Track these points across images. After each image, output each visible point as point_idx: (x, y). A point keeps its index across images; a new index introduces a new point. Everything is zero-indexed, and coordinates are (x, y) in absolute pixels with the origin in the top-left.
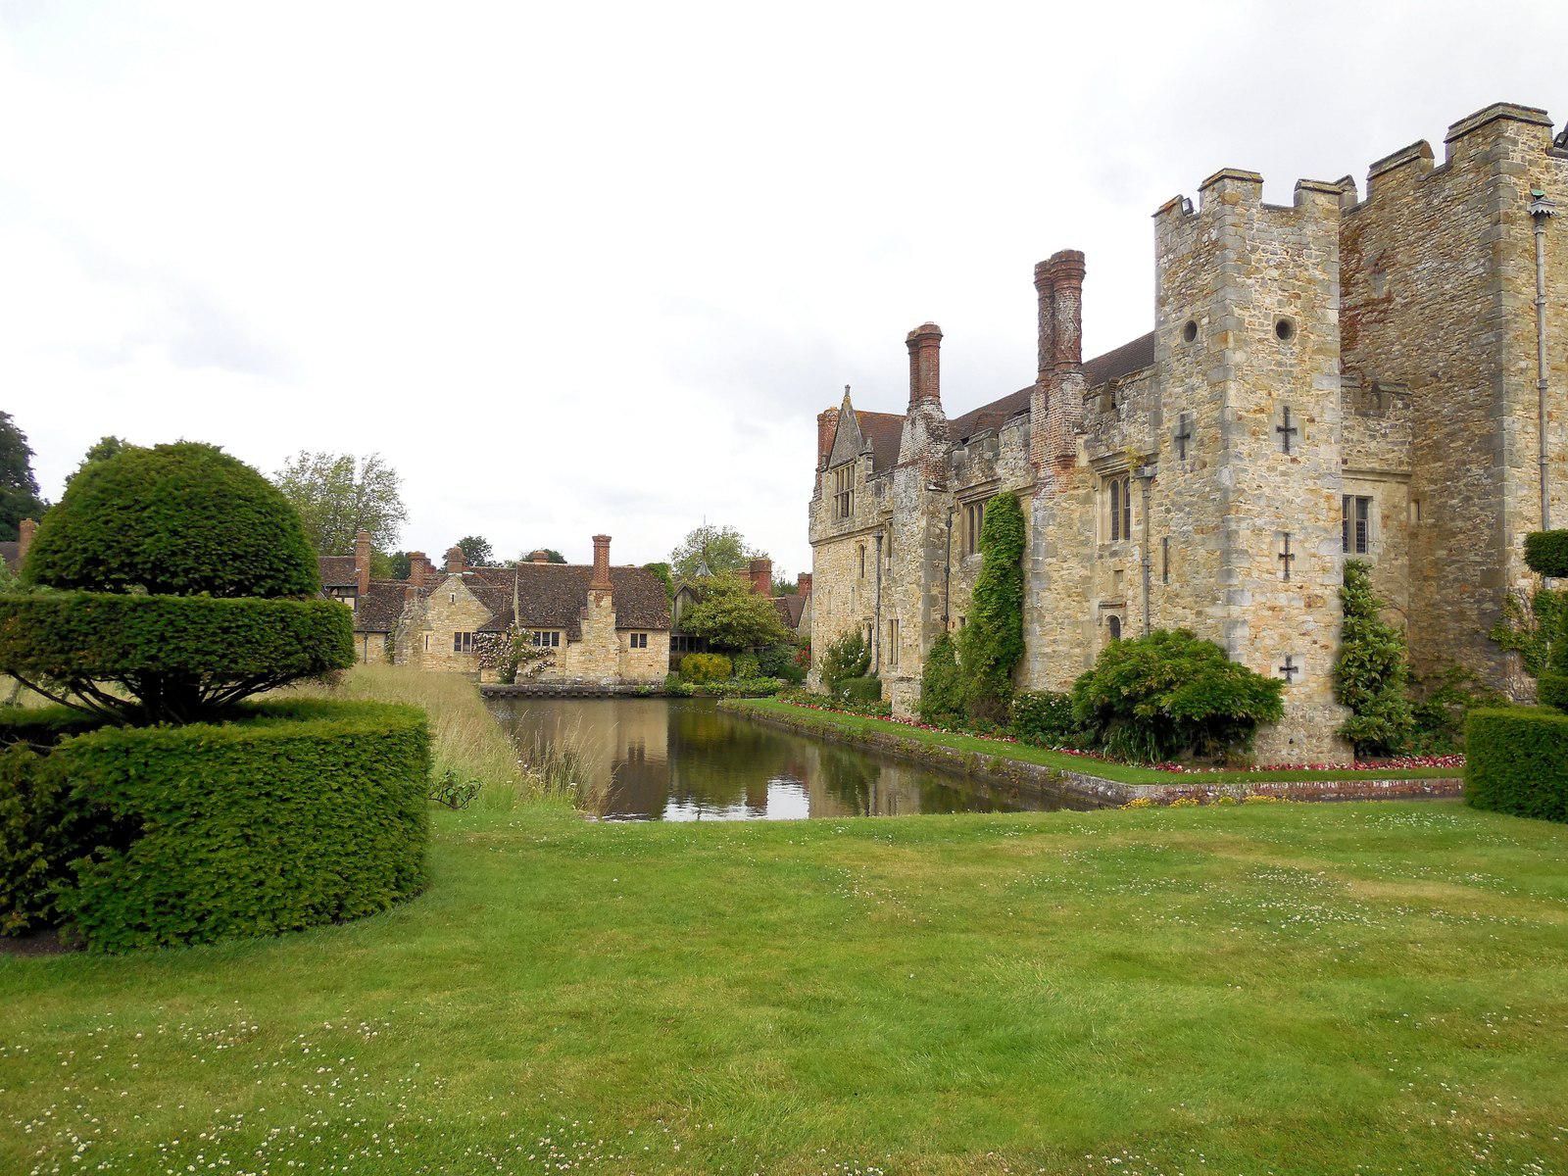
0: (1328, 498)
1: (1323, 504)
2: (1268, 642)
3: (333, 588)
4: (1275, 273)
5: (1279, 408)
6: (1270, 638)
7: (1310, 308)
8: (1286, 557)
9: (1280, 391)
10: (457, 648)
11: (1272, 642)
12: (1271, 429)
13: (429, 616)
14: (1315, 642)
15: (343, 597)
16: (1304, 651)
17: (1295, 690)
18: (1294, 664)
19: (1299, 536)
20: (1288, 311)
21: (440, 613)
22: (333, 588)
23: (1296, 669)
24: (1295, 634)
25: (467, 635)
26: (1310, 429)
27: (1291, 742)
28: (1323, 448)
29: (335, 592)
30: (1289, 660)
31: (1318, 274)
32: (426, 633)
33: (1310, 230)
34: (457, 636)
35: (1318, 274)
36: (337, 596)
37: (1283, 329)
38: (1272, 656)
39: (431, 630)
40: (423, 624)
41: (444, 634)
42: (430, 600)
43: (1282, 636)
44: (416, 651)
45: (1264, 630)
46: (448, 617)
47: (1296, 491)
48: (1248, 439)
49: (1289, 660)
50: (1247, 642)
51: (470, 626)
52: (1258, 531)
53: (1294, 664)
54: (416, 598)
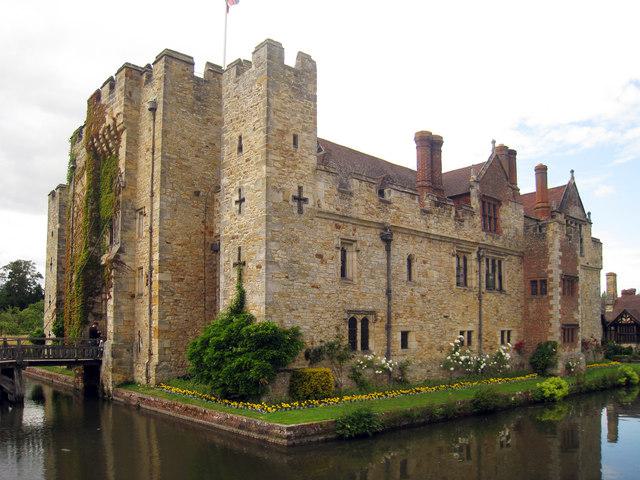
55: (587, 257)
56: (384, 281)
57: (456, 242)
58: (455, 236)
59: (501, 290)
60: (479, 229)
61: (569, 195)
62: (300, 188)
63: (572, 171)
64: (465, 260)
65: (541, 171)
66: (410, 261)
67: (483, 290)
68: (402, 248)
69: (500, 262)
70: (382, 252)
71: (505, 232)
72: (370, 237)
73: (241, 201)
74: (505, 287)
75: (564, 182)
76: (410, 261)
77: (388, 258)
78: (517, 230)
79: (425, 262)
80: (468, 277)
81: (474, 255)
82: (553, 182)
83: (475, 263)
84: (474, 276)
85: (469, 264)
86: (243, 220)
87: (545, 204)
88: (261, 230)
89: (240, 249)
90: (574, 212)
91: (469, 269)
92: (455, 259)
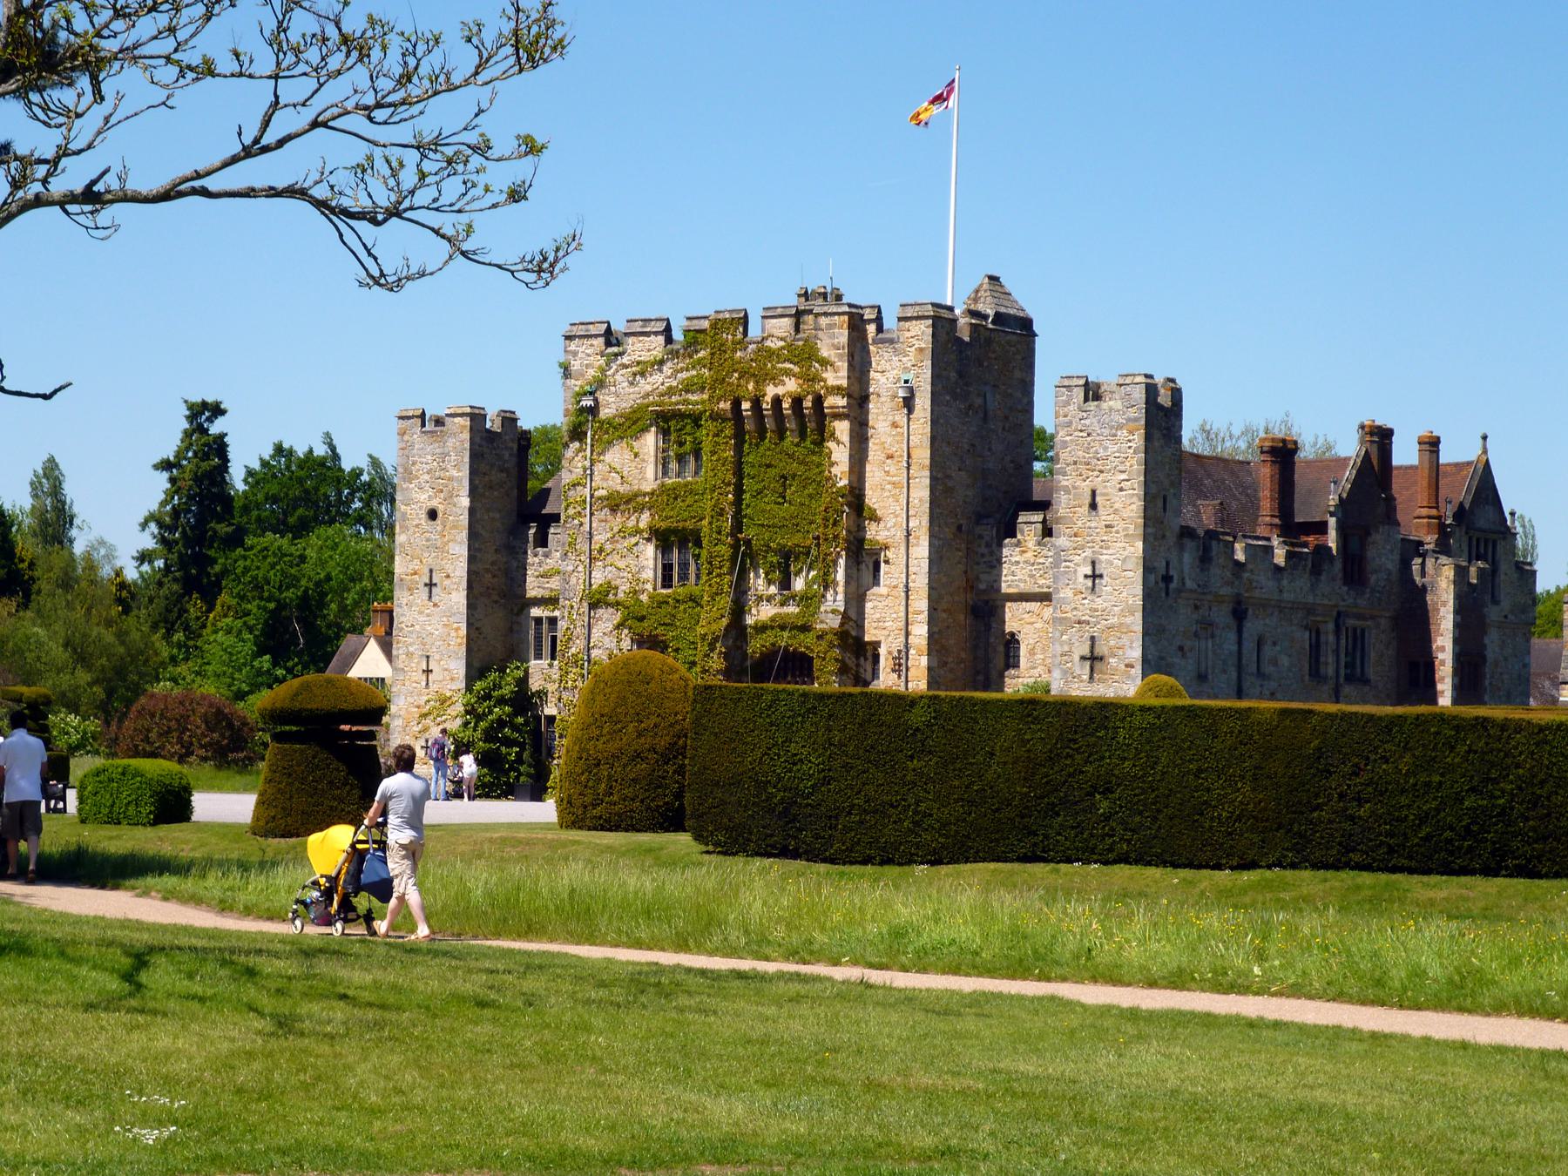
0: (457, 629)
1: (453, 634)
4: (427, 477)
5: (427, 571)
7: (450, 497)
8: (428, 671)
9: (430, 560)
12: (421, 586)
19: (437, 657)
20: (434, 503)
26: (447, 582)
28: (454, 594)
31: (455, 473)
33: (451, 442)
35: (455, 473)
37: (433, 515)
47: (435, 627)
48: (406, 593)
52: (409, 655)
55: (1506, 604)
56: (1234, 675)
57: (1310, 610)
58: (1310, 599)
59: (1366, 682)
60: (1339, 582)
61: (1485, 487)
62: (1168, 564)
63: (1485, 438)
64: (1318, 632)
65: (1431, 445)
66: (1260, 643)
67: (1342, 680)
68: (1252, 627)
69: (1363, 631)
70: (1232, 636)
71: (1373, 578)
72: (1222, 615)
73: (1095, 576)
74: (1371, 673)
75: (1470, 453)
76: (1260, 643)
77: (1240, 643)
78: (1390, 574)
79: (1275, 644)
80: (1322, 659)
81: (1331, 626)
82: (1447, 456)
83: (1331, 638)
84: (1331, 659)
85: (1323, 638)
86: (1099, 603)
87: (1434, 512)
88: (1136, 622)
89: (1093, 638)
90: (1483, 520)
91: (1323, 647)
92: (1307, 634)
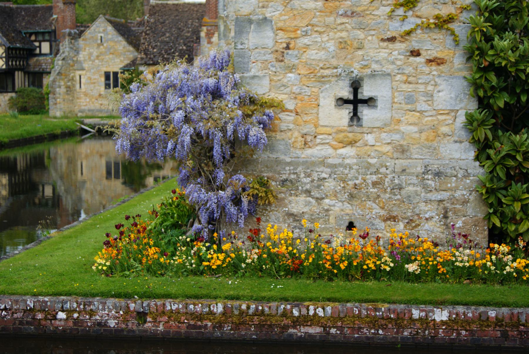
2: (313, 54)
3: (31, 34)
6: (319, 49)
10: (107, 86)
11: (322, 55)
13: (81, 56)
14: (416, 53)
15: (40, 42)
16: (389, 68)
17: (370, 138)
18: (366, 92)
21: (90, 54)
22: (31, 34)
23: (370, 102)
24: (371, 41)
25: (116, 74)
27: (351, 226)
29: (33, 38)
30: (356, 86)
32: (78, 73)
34: (107, 76)
36: (35, 41)
38: (322, 80)
39: (83, 69)
40: (73, 64)
41: (94, 74)
42: (81, 42)
43: (343, 45)
44: (70, 90)
45: (306, 34)
46: (98, 57)
49: (356, 86)
50: (271, 57)
51: (116, 65)
53: (366, 92)
54: (67, 40)
